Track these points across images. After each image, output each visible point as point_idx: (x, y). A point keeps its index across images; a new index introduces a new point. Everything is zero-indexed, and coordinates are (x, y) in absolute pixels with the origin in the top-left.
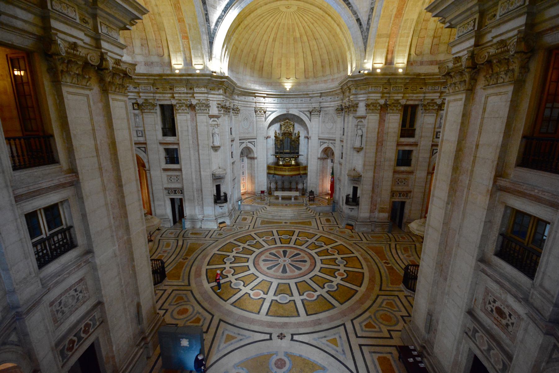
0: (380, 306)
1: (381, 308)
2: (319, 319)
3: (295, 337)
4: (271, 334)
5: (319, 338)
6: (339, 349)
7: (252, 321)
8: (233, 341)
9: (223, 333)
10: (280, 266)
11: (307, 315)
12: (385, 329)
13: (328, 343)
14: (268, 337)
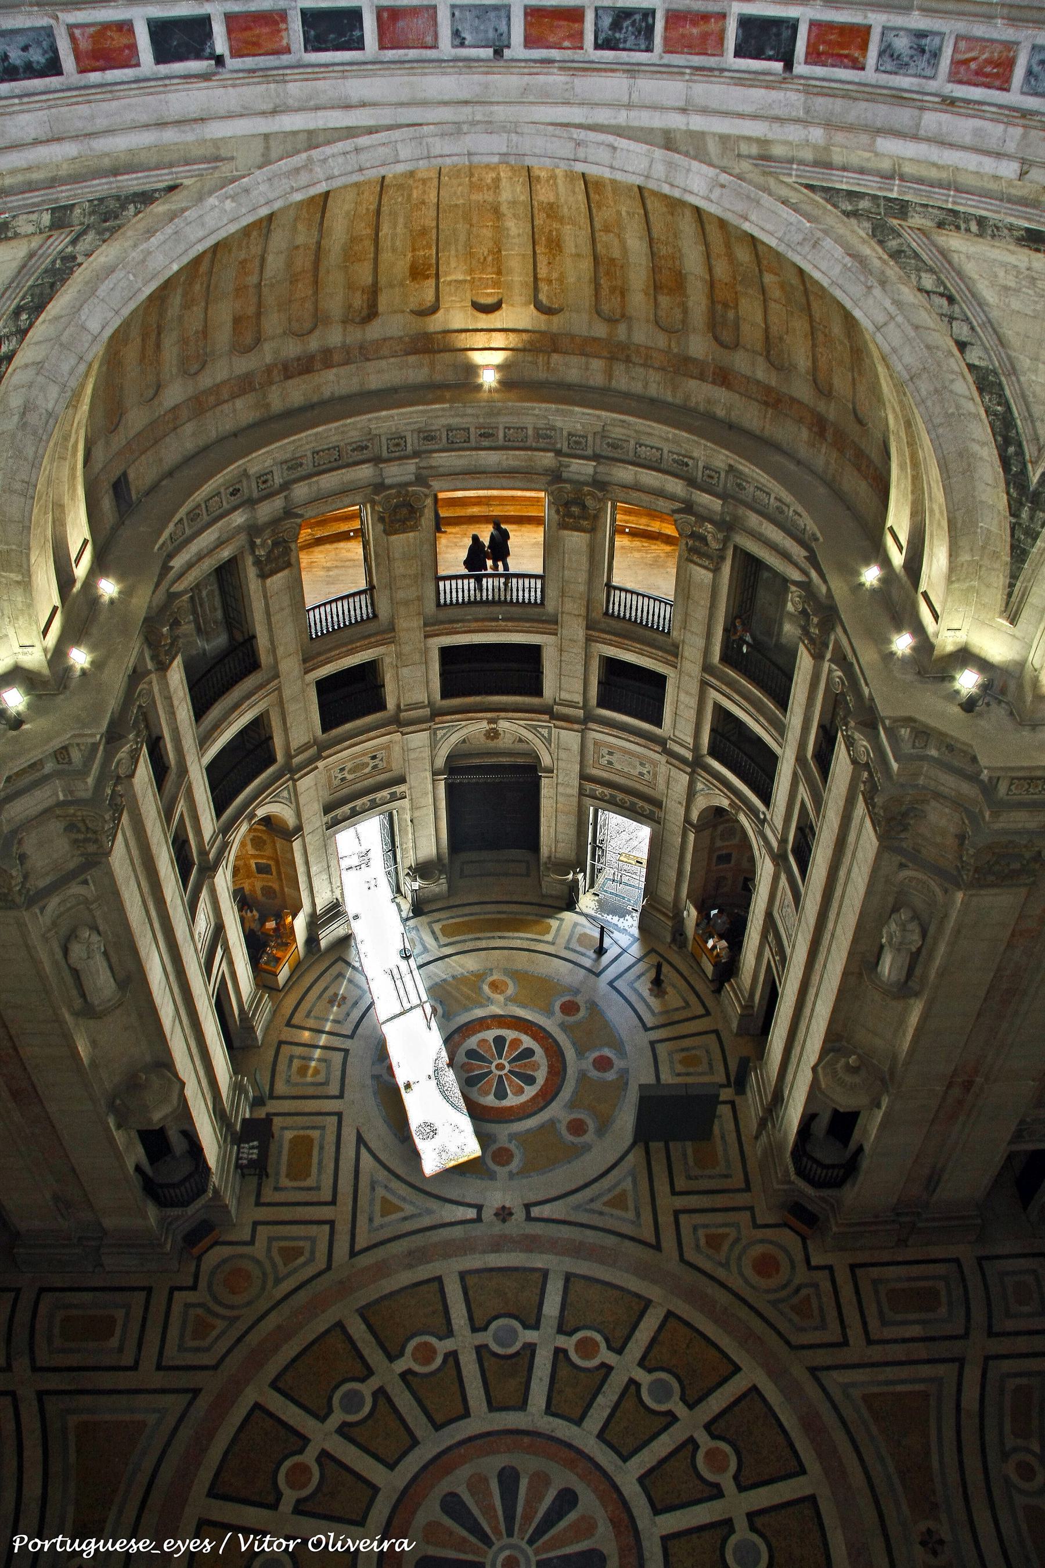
0: (233, 1320)
1: (235, 1313)
2: (410, 1266)
3: (471, 1213)
4: (529, 1218)
5: (420, 1215)
6: (380, 1192)
7: (576, 1250)
8: (610, 1196)
9: (638, 1215)
10: (527, 1518)
11: (439, 1279)
12: (259, 1249)
13: (402, 1204)
14: (535, 1212)
